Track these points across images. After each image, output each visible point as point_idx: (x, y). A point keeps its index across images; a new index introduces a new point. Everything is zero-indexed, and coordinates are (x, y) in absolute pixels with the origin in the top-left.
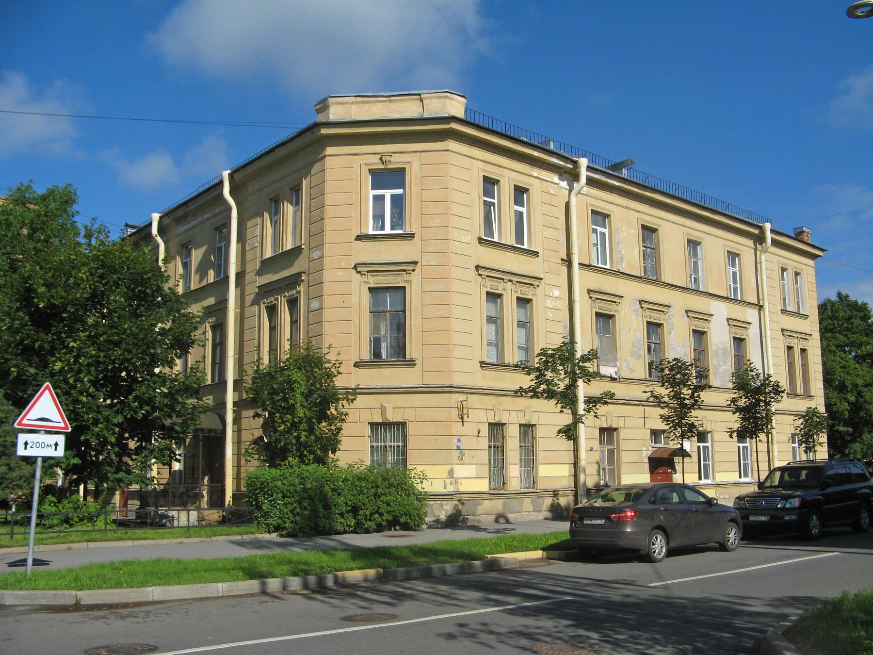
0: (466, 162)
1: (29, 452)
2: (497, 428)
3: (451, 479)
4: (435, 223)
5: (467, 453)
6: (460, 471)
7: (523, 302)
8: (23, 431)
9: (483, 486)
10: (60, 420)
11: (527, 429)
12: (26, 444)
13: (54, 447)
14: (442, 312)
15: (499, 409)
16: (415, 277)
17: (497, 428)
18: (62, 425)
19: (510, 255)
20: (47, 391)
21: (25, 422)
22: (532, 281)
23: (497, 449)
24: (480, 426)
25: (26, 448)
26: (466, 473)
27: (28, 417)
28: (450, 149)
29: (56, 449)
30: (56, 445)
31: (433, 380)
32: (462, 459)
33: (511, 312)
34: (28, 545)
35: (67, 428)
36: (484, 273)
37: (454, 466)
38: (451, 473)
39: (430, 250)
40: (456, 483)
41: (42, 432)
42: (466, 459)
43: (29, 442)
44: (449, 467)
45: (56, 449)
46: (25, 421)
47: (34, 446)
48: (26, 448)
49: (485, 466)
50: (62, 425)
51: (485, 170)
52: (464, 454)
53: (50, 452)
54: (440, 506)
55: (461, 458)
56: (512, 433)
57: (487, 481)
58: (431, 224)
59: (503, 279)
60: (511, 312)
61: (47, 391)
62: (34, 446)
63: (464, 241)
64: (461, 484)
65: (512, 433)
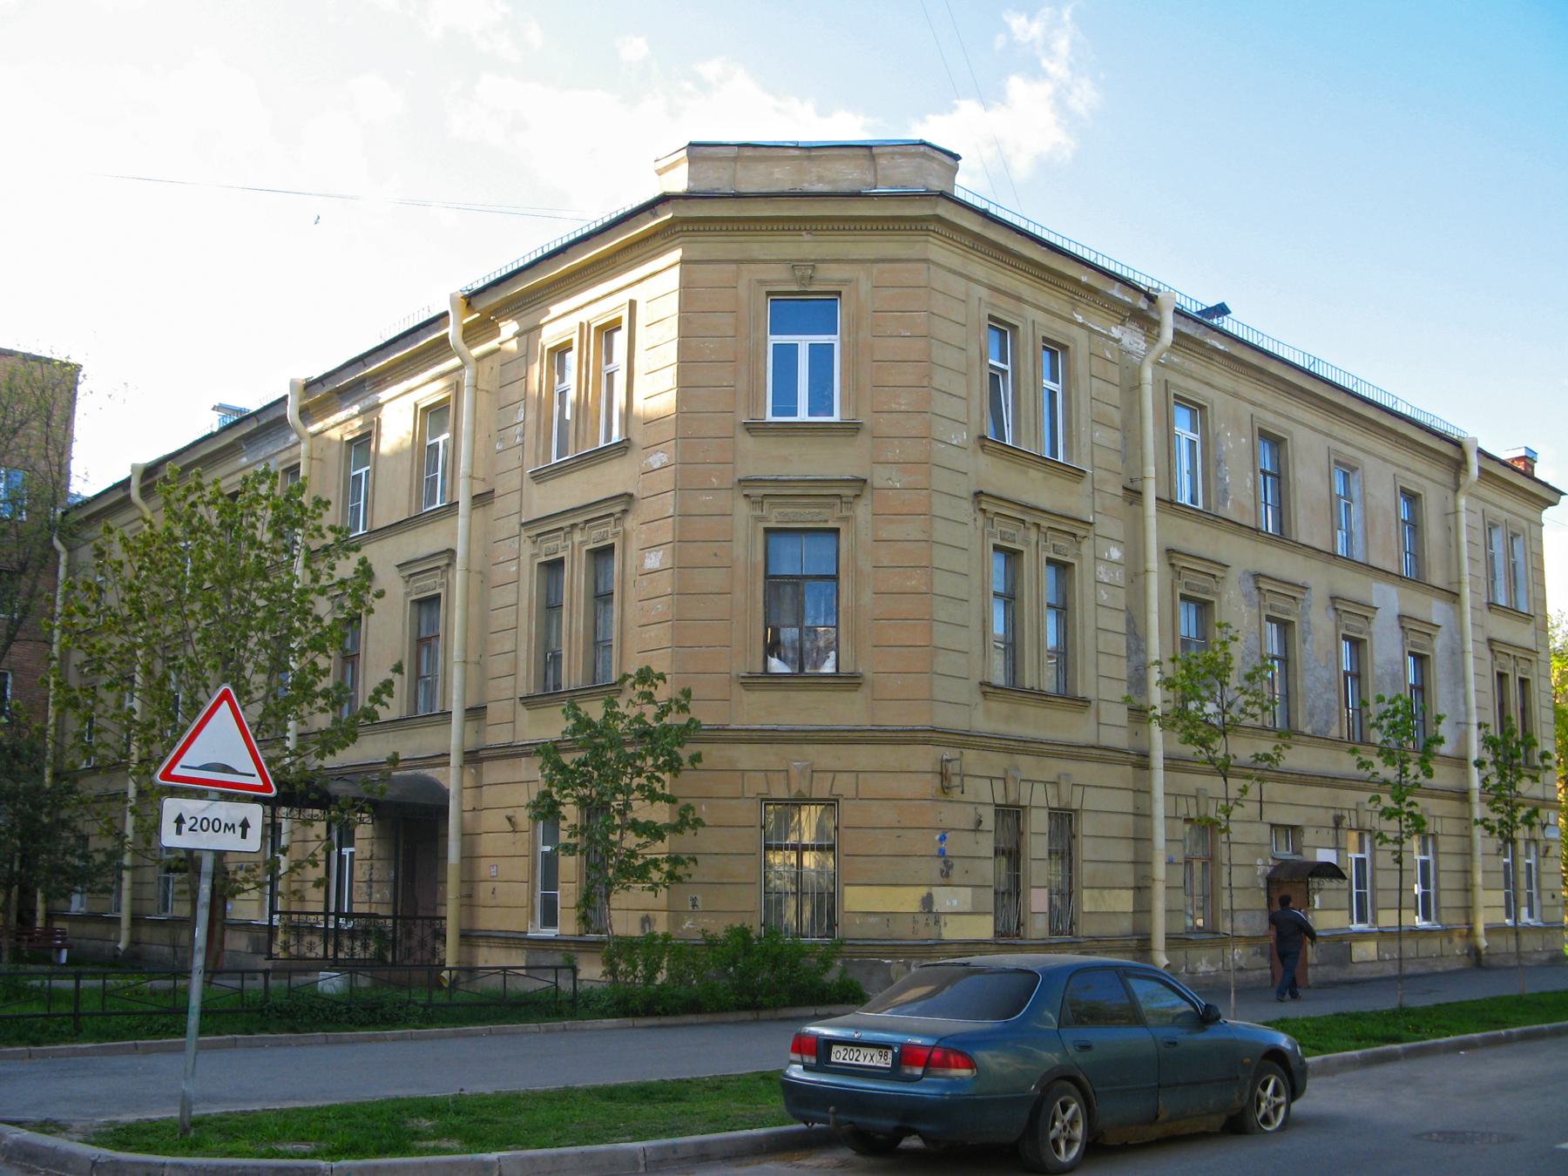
0: (959, 286)
1: (186, 841)
2: (1011, 814)
3: (927, 916)
4: (901, 404)
5: (957, 864)
6: (947, 899)
7: (1062, 568)
8: (174, 792)
9: (983, 928)
10: (254, 770)
11: (1064, 820)
12: (180, 820)
13: (239, 830)
14: (913, 582)
15: (1015, 779)
16: (862, 511)
17: (1011, 814)
18: (258, 781)
19: (1035, 474)
20: (225, 704)
21: (177, 771)
22: (1075, 527)
23: (1011, 854)
24: (981, 810)
25: (179, 832)
26: (955, 902)
27: (183, 761)
28: (931, 256)
29: (244, 836)
30: (245, 825)
31: (893, 717)
32: (947, 875)
33: (1039, 583)
34: (183, 1033)
35: (266, 787)
36: (991, 508)
37: (934, 889)
38: (928, 901)
39: (890, 456)
40: (937, 922)
41: (215, 796)
42: (956, 875)
43: (186, 818)
44: (923, 891)
45: (244, 836)
46: (177, 771)
47: (197, 827)
48: (179, 832)
49: (988, 889)
50: (258, 781)
51: (994, 305)
52: (952, 865)
53: (229, 842)
54: (905, 968)
55: (946, 873)
56: (1038, 823)
57: (990, 919)
58: (893, 406)
59: (1023, 521)
60: (1039, 583)
61: (225, 704)
62: (197, 827)
63: (955, 442)
64: (945, 924)
65: (1038, 823)
